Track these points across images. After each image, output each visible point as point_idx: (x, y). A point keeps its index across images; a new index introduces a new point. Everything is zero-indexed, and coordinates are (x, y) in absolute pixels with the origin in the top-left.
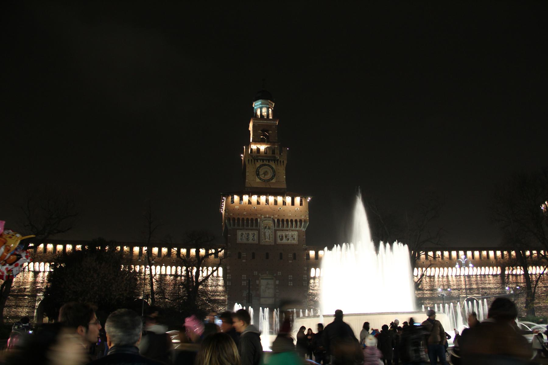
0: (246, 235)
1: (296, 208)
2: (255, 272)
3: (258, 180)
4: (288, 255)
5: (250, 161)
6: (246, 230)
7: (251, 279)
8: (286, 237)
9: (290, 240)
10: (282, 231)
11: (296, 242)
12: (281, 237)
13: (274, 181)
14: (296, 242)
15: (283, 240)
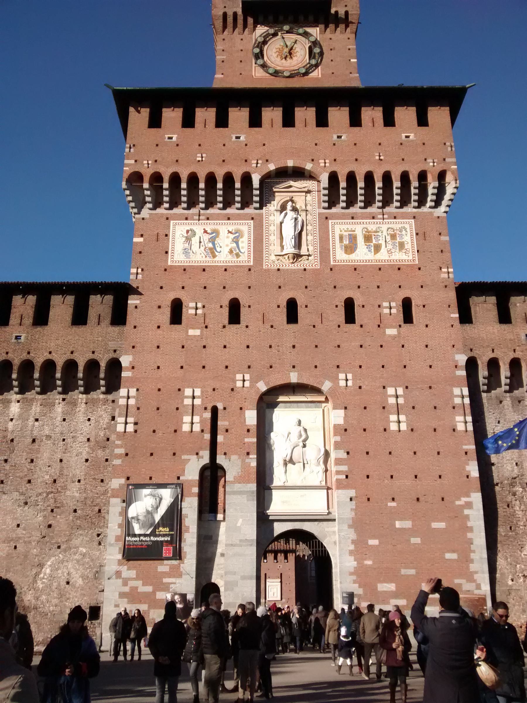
0: (206, 237)
1: (404, 135)
2: (239, 377)
3: (258, 73)
4: (379, 306)
5: (230, 20)
6: (208, 219)
7: (220, 406)
8: (368, 238)
9: (383, 250)
10: (353, 218)
11: (411, 258)
12: (346, 242)
13: (316, 74)
14: (411, 258)
15: (356, 252)
